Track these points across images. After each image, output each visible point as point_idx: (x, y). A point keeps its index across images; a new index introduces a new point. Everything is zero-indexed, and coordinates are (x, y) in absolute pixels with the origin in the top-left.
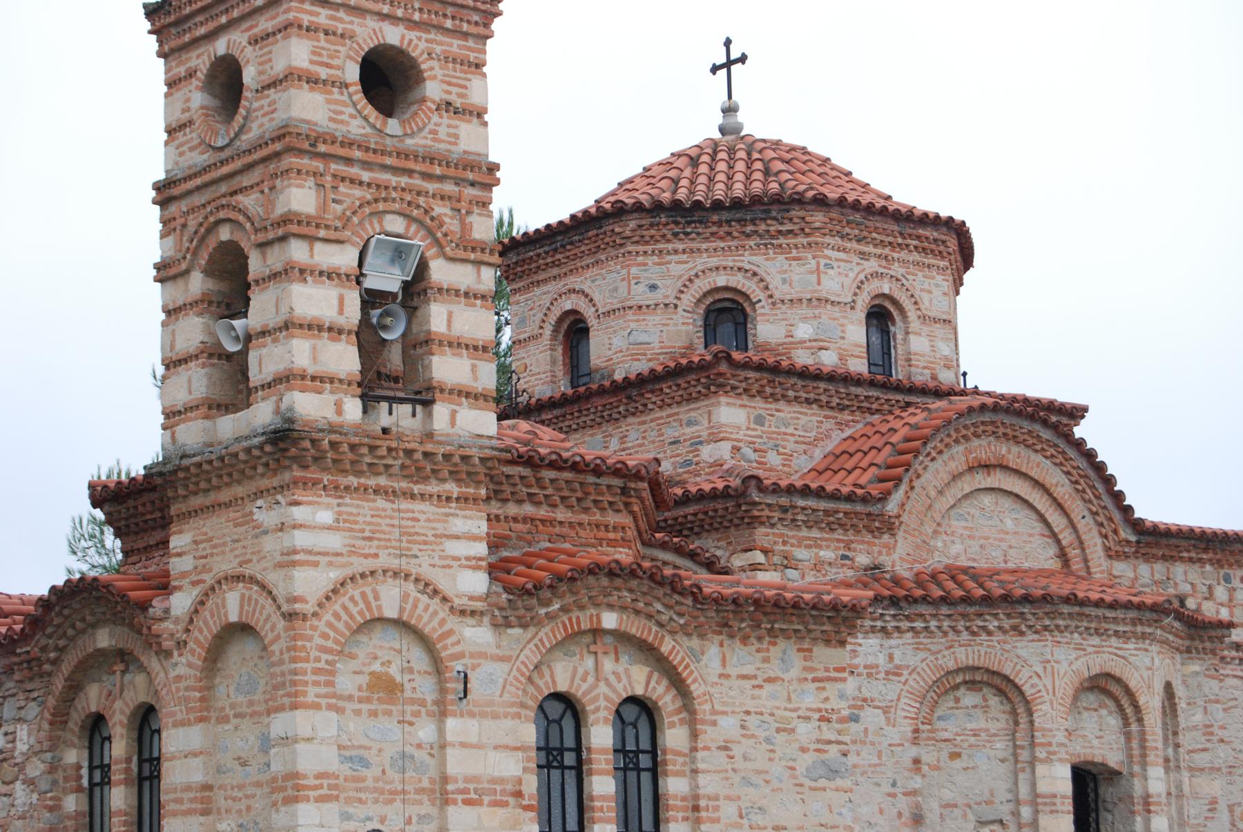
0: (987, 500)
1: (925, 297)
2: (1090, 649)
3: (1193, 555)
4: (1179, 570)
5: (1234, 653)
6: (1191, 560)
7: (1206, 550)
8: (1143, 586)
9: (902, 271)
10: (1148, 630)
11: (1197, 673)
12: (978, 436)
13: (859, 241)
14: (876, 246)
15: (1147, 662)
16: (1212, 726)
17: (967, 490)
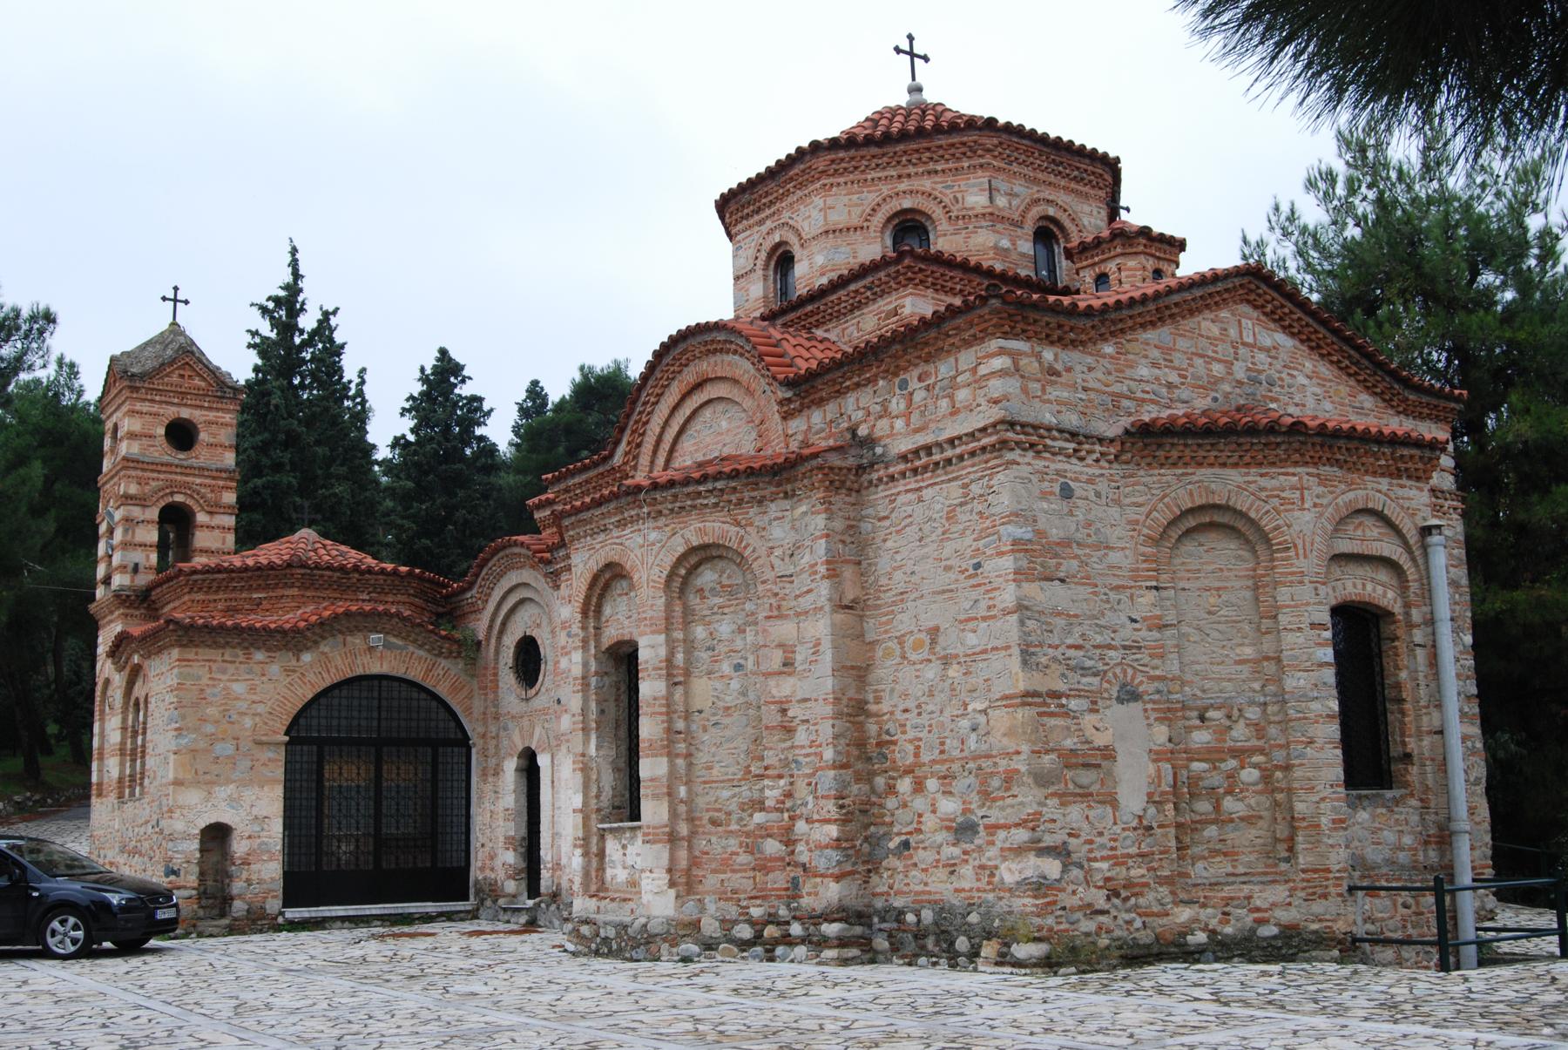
0: (707, 413)
1: (806, 225)
2: (598, 546)
3: (856, 379)
4: (850, 401)
5: (902, 467)
6: (858, 385)
7: (861, 371)
8: (817, 433)
9: (789, 214)
10: (633, 513)
11: (805, 513)
12: (686, 365)
13: (757, 212)
14: (769, 207)
15: (640, 540)
16: (816, 564)
17: (688, 412)
